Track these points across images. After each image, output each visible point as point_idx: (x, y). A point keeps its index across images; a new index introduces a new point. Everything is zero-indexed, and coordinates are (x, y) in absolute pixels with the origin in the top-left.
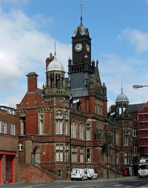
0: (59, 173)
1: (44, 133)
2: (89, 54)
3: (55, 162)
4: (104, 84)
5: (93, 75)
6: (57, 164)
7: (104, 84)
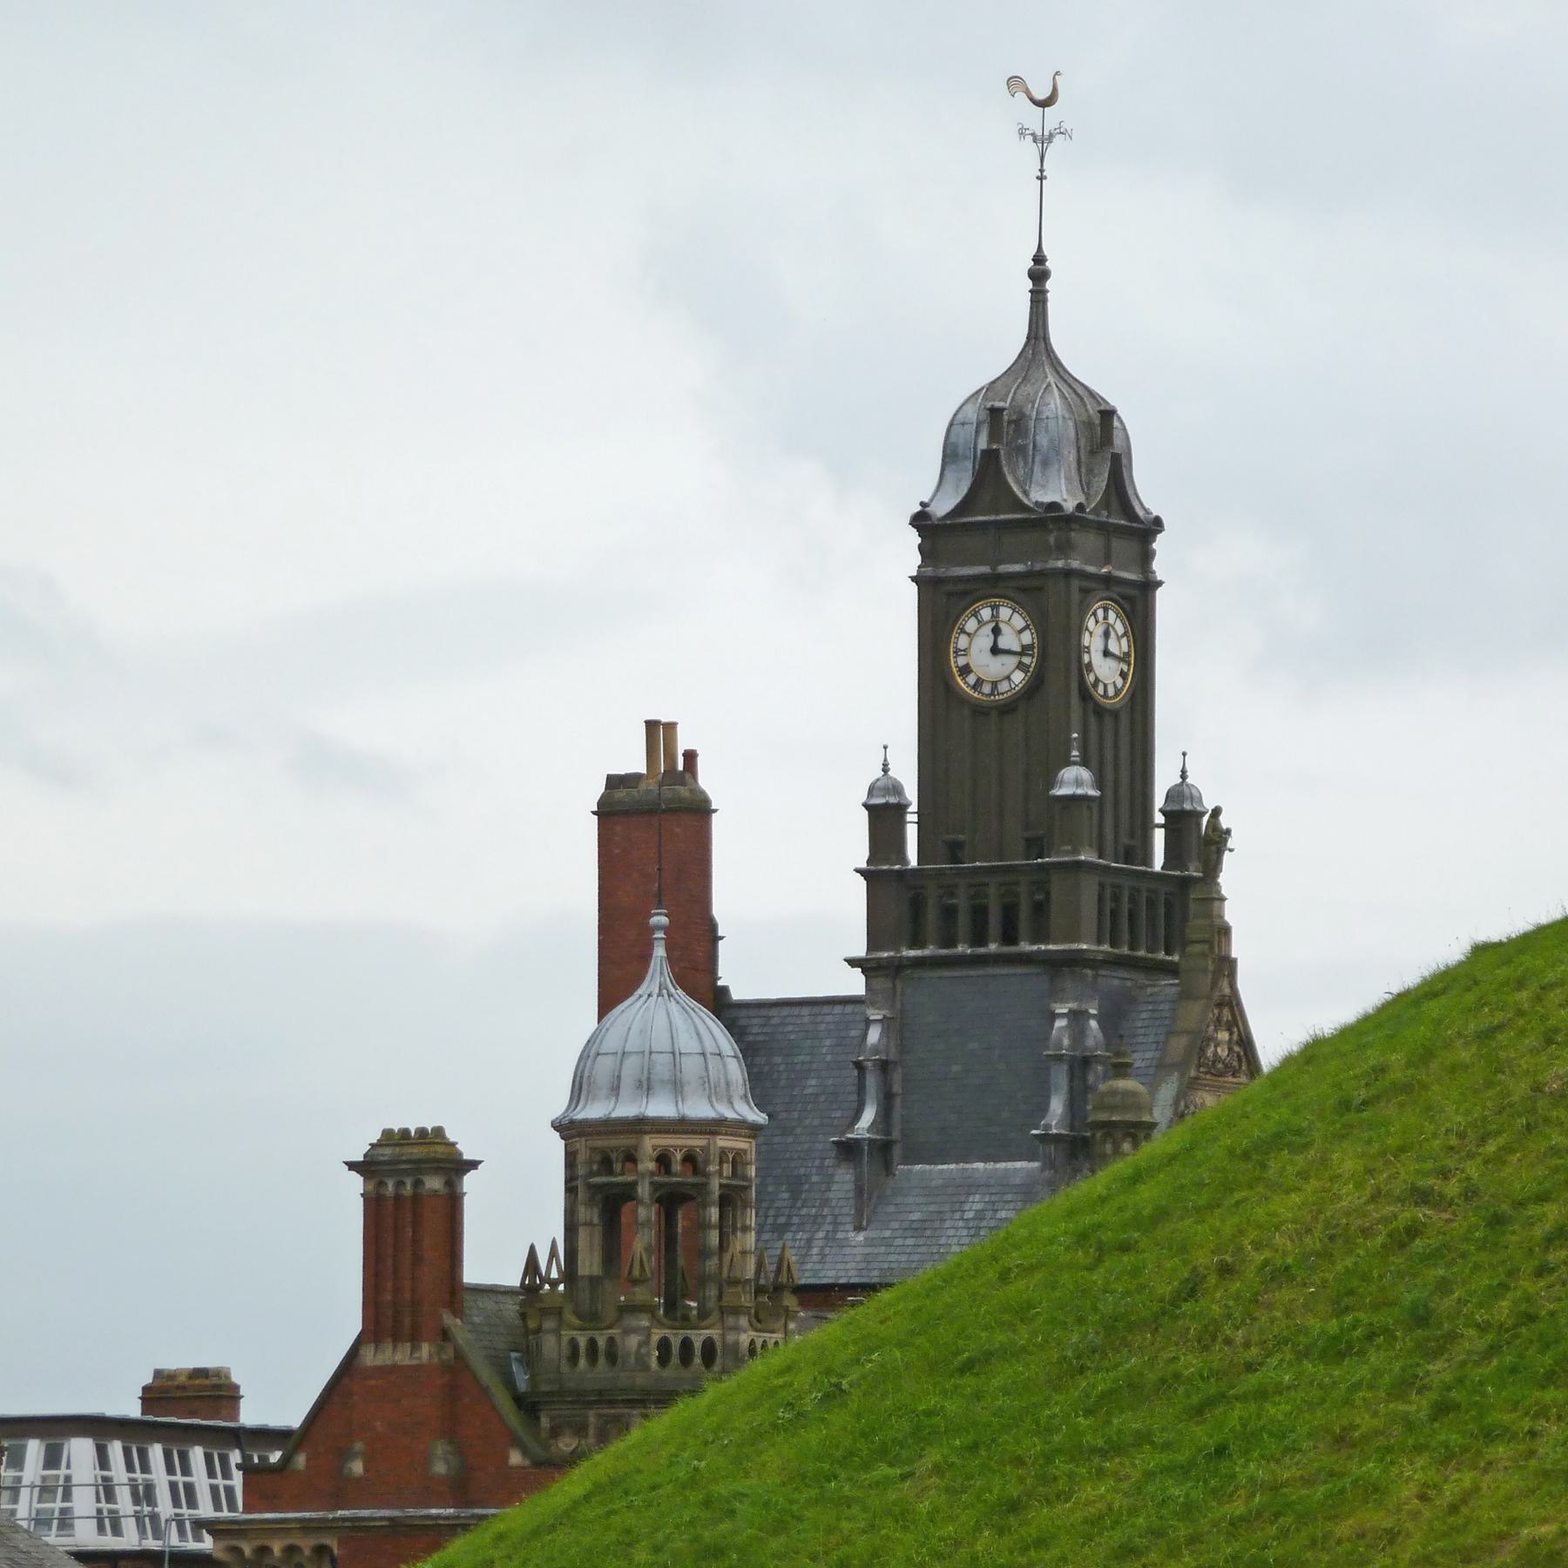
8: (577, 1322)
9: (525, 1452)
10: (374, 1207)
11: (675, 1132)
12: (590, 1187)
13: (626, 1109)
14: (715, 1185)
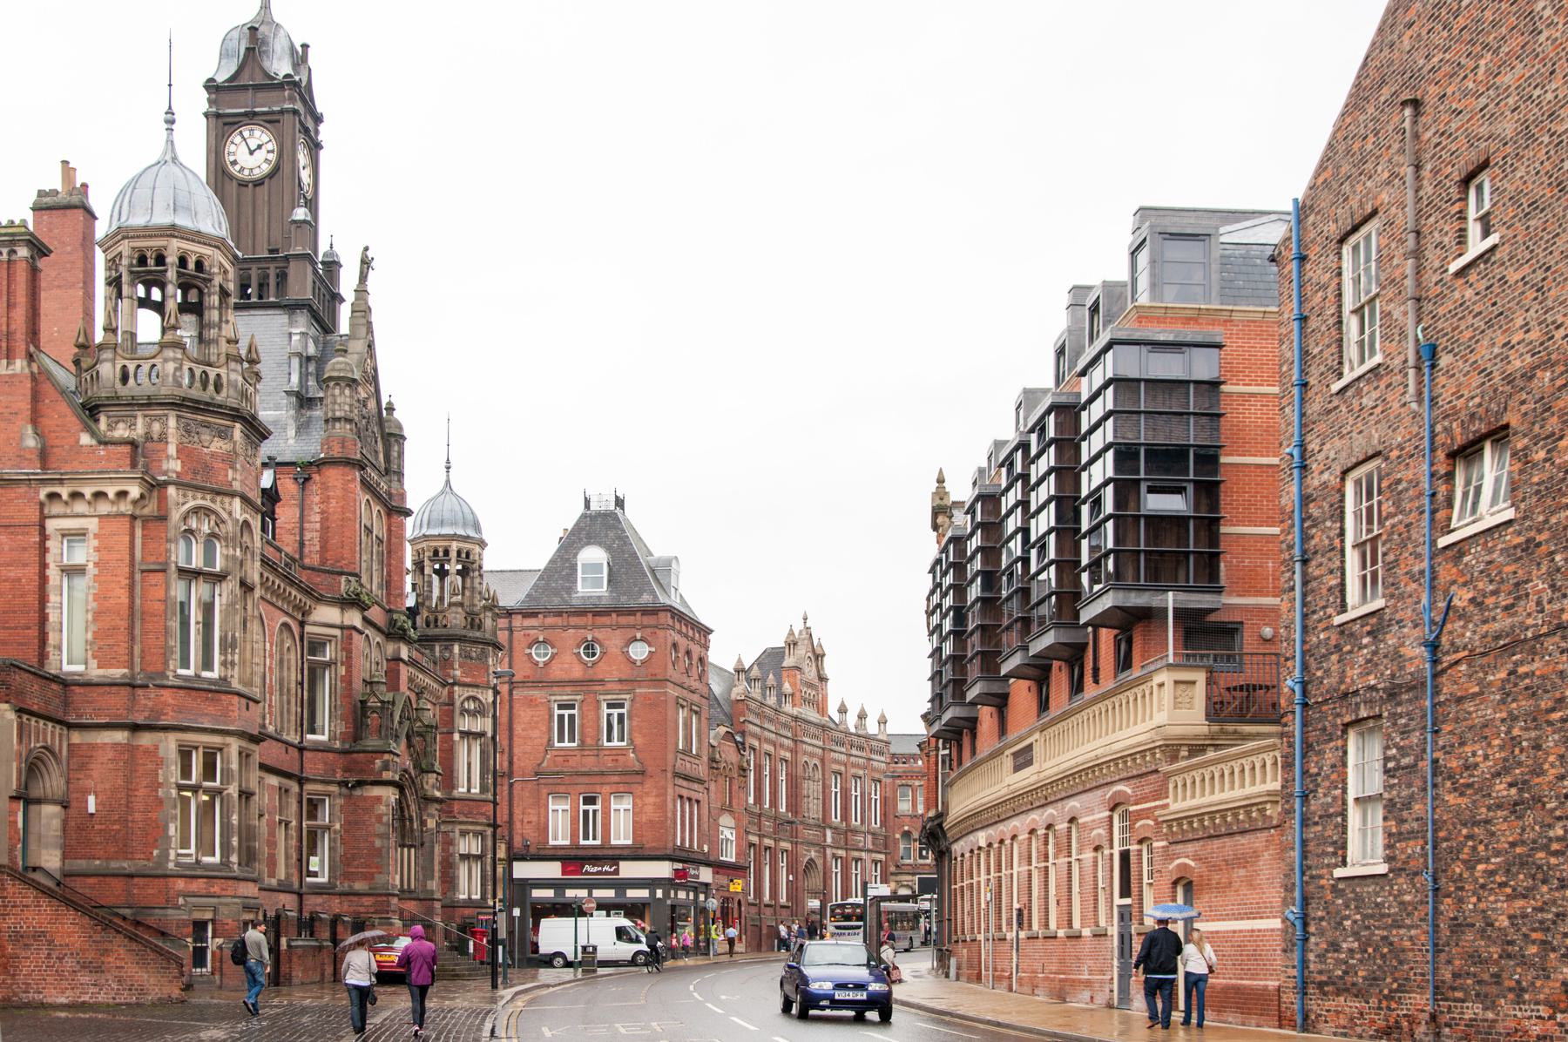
0: (195, 941)
1: (93, 663)
3: (171, 865)
6: (180, 884)
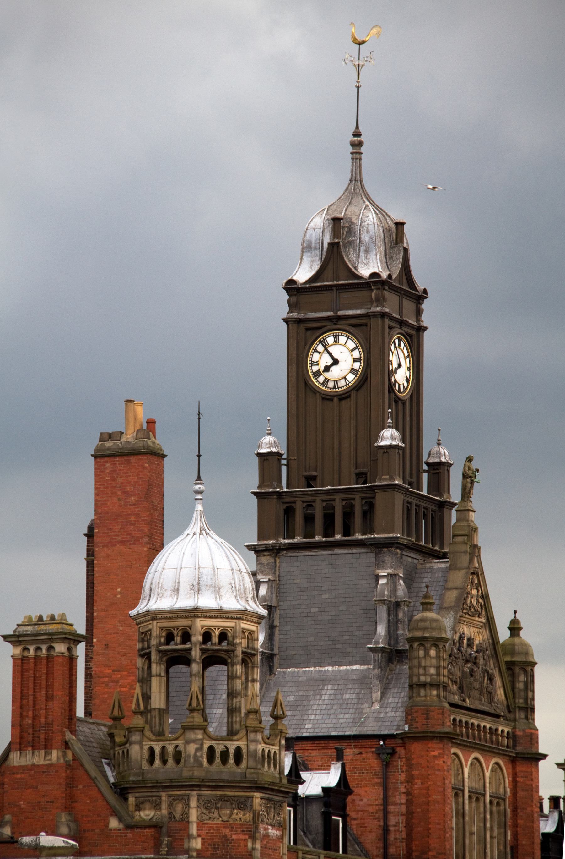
2: (409, 410)
4: (515, 628)
5: (439, 565)
7: (515, 628)
8: (154, 738)
9: (120, 820)
10: (21, 666)
11: (216, 617)
12: (160, 651)
13: (185, 602)
14: (239, 651)
